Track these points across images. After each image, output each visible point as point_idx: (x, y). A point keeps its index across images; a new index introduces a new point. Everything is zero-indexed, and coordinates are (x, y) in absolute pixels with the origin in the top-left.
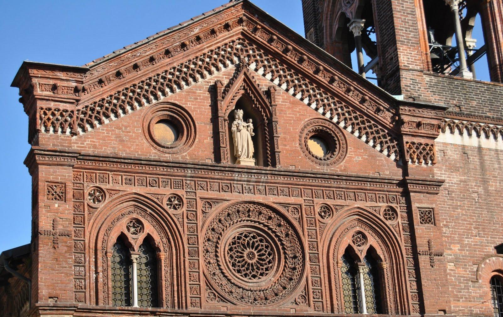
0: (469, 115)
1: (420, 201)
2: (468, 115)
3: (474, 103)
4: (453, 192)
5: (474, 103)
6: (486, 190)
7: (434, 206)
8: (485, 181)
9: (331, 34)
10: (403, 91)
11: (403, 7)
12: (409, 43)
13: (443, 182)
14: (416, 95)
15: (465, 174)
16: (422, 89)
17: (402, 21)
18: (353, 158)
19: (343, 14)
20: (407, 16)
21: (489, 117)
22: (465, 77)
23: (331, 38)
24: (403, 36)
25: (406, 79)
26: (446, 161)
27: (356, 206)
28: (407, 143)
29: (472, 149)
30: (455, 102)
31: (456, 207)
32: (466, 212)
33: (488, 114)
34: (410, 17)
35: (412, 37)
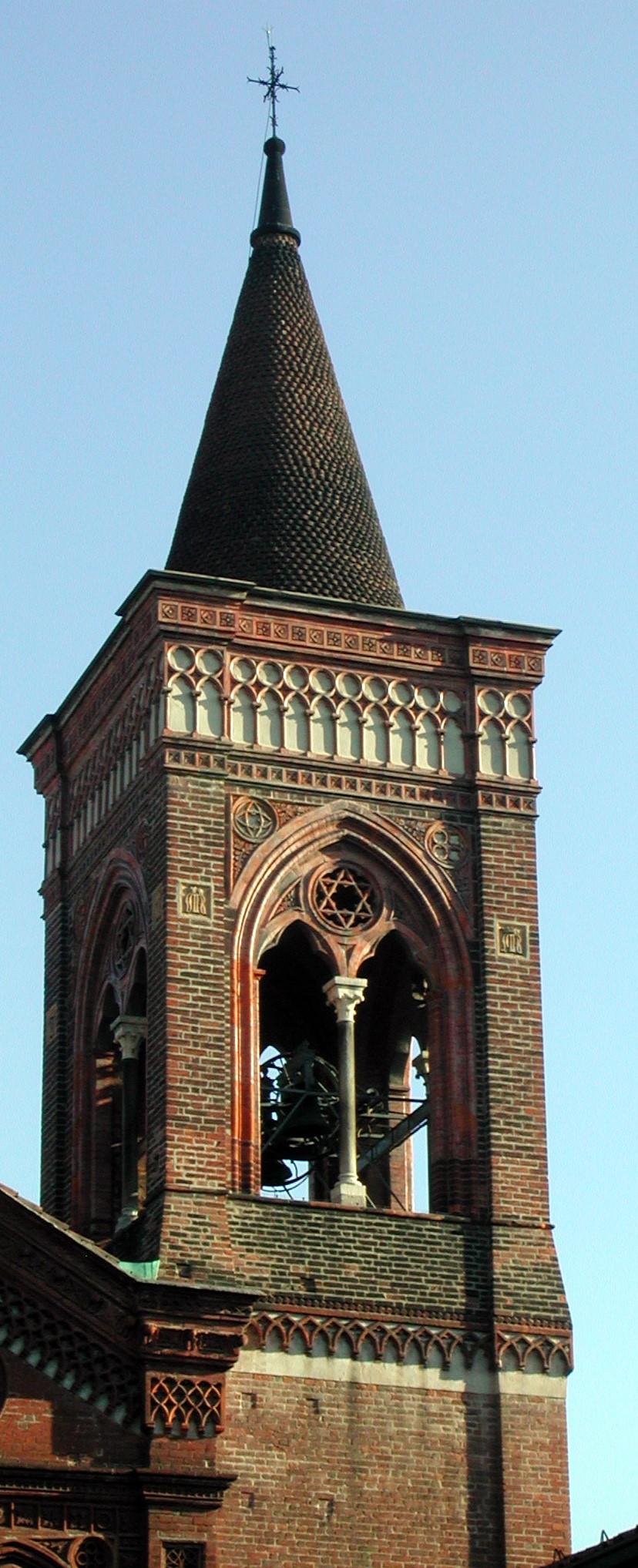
0: (335, 1300)
1: (171, 1528)
2: (332, 1303)
3: (353, 1271)
4: (264, 1499)
5: (353, 1271)
6: (356, 1492)
7: (205, 1538)
8: (354, 1470)
9: (88, 1030)
10: (166, 1249)
11: (194, 1029)
12: (198, 1121)
13: (233, 1478)
14: (195, 1255)
15: (304, 1452)
16: (216, 1241)
17: (189, 1067)
18: (18, 1418)
19: (111, 989)
20: (203, 1053)
21: (386, 1305)
22: (346, 1203)
23: (87, 1042)
24: (186, 1105)
25: (178, 1211)
26: (259, 1420)
27: (8, 1538)
28: (155, 1381)
29: (333, 1386)
30: (301, 1269)
31: (269, 1537)
32: (293, 1550)
33: (386, 1298)
34: (210, 1055)
35: (210, 1107)
